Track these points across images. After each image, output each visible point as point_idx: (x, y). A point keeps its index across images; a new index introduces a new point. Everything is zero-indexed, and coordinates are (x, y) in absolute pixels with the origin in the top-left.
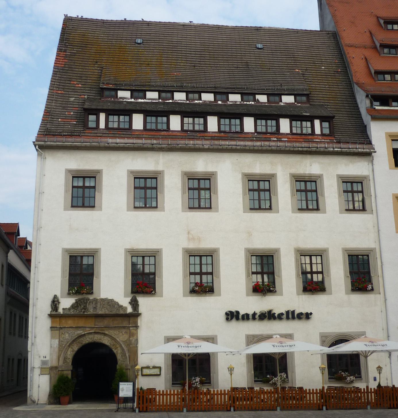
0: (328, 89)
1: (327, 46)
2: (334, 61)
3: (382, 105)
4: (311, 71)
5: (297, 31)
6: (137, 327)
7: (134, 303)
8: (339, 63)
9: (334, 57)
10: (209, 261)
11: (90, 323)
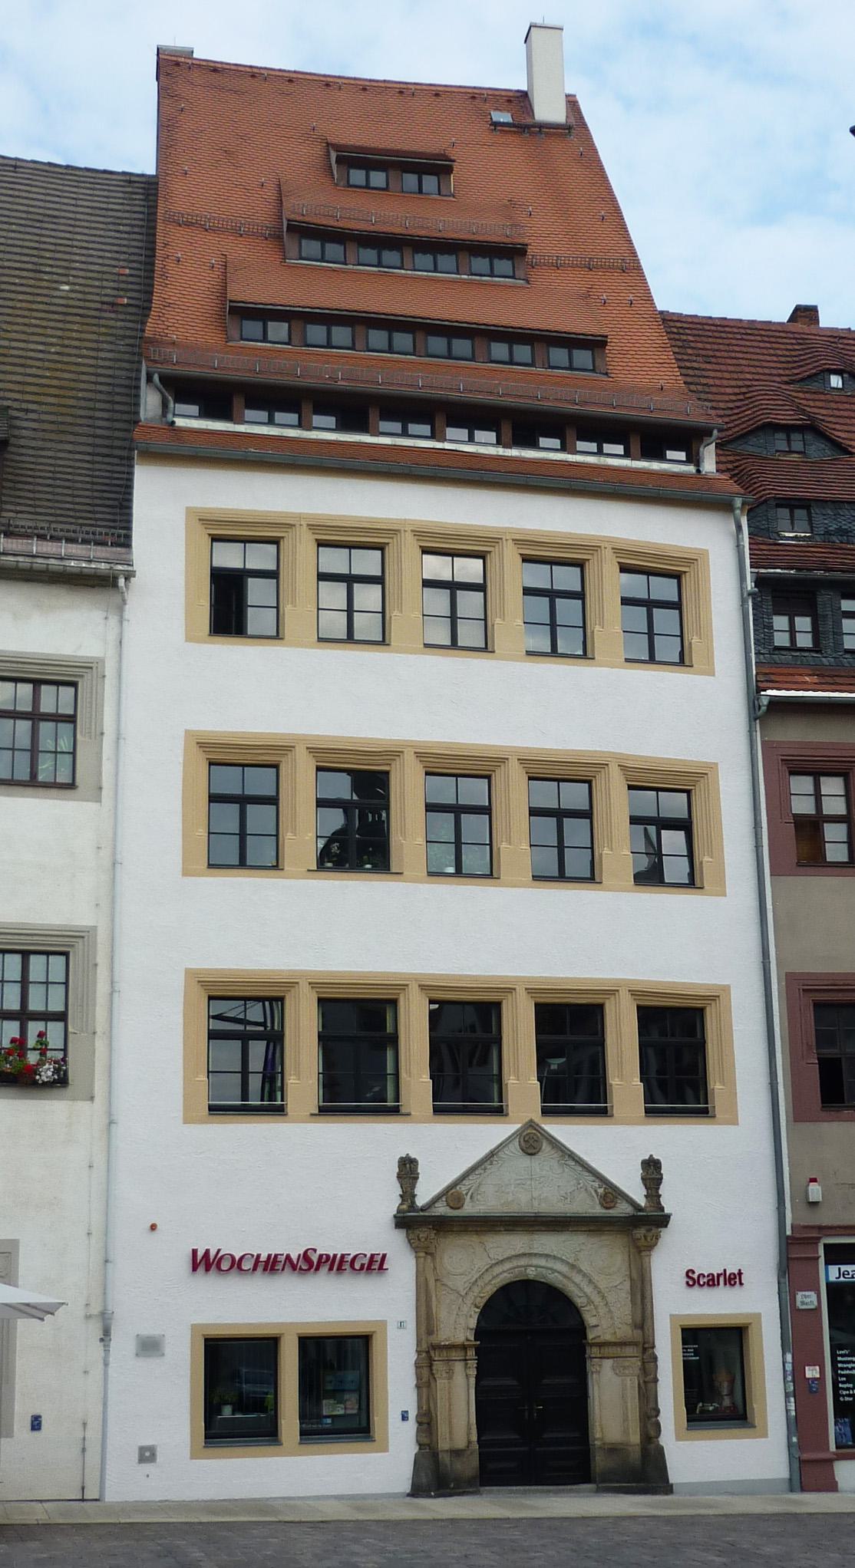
0: (56, 357)
1: (109, 220)
2: (116, 270)
3: (209, 411)
4: (12, 296)
5: (13, 163)
8: (131, 279)
9: (122, 257)
10: (57, 974)
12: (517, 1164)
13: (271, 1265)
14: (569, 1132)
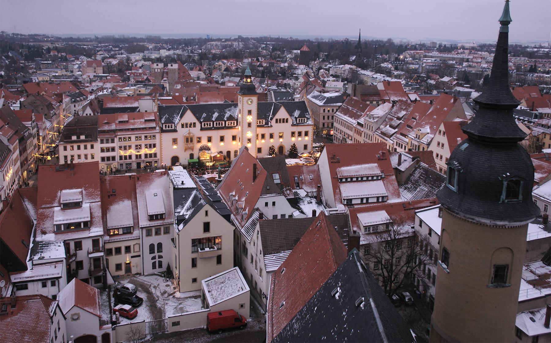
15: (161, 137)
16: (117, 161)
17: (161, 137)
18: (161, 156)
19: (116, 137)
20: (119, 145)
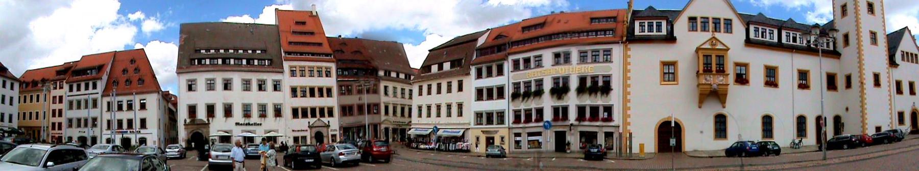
6: (209, 127)
7: (208, 120)
11: (195, 126)
12: (318, 122)
13: (299, 131)
14: (322, 119)
15: (626, 56)
16: (507, 125)
17: (626, 56)
18: (625, 116)
19: (505, 58)
20: (512, 81)
